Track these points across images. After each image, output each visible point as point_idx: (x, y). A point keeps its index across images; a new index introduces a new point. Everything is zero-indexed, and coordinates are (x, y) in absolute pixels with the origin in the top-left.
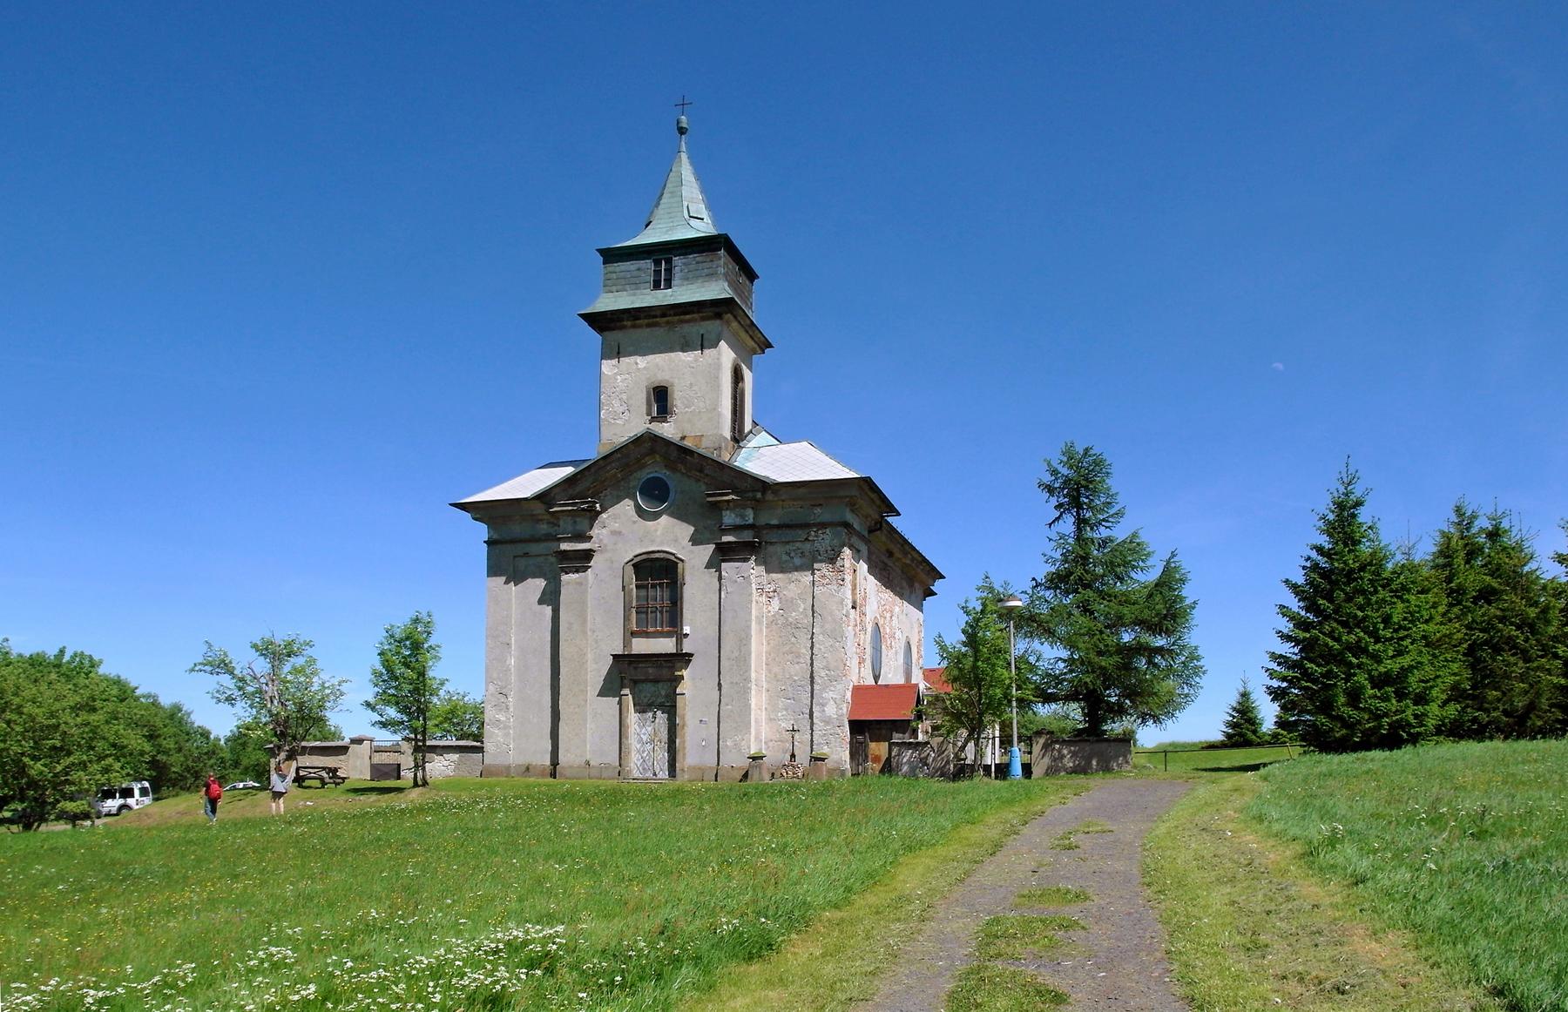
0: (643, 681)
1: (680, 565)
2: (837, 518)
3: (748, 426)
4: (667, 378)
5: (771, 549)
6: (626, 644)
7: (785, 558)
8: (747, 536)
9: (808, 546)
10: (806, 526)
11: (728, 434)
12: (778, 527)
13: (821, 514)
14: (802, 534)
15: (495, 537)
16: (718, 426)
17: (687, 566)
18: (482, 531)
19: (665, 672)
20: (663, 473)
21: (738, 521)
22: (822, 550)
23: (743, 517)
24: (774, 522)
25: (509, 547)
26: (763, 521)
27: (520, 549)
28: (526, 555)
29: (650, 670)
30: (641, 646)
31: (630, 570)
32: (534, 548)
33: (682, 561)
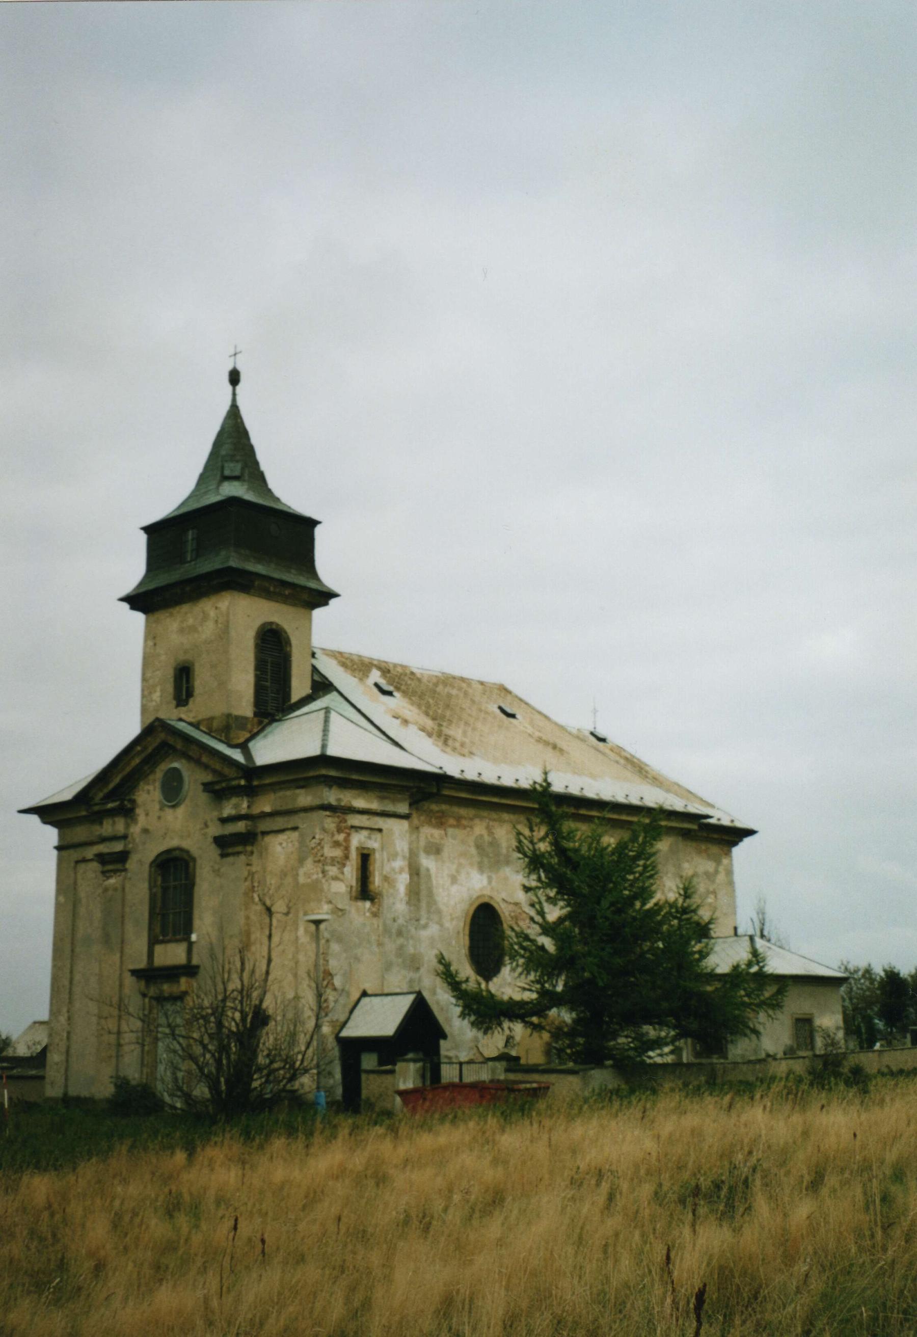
3: (300, 687)
5: (268, 839)
12: (272, 814)
13: (304, 798)
17: (199, 862)
18: (51, 835)
24: (267, 809)
26: (256, 810)
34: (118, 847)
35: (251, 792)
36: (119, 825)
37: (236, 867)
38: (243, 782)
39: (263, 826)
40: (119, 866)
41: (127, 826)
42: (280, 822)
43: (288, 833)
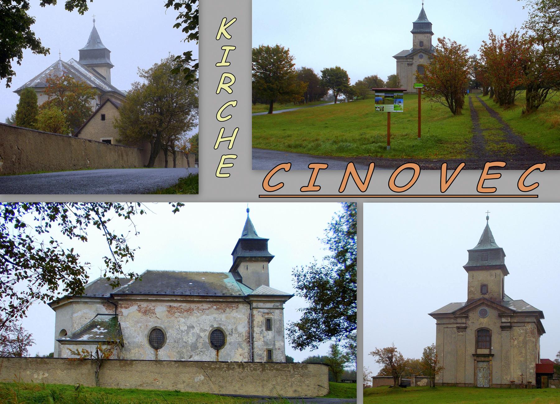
0: (480, 361)
1: (490, 331)
2: (532, 321)
4: (486, 283)
5: (514, 328)
6: (476, 351)
7: (518, 330)
8: (509, 324)
9: (524, 328)
10: (525, 322)
11: (501, 298)
12: (517, 322)
13: (528, 320)
14: (523, 324)
15: (439, 322)
16: (500, 297)
17: (493, 331)
18: (435, 321)
19: (486, 359)
20: (486, 308)
21: (506, 321)
22: (528, 328)
23: (507, 320)
24: (515, 321)
25: (443, 325)
26: (512, 321)
27: (445, 326)
28: (447, 327)
29: (482, 359)
30: (480, 351)
31: (476, 332)
32: (449, 326)
33: (491, 330)
34: (464, 325)
35: (511, 317)
36: (464, 320)
37: (505, 333)
38: (512, 314)
39: (513, 325)
40: (464, 330)
41: (466, 321)
42: (519, 324)
43: (522, 327)
